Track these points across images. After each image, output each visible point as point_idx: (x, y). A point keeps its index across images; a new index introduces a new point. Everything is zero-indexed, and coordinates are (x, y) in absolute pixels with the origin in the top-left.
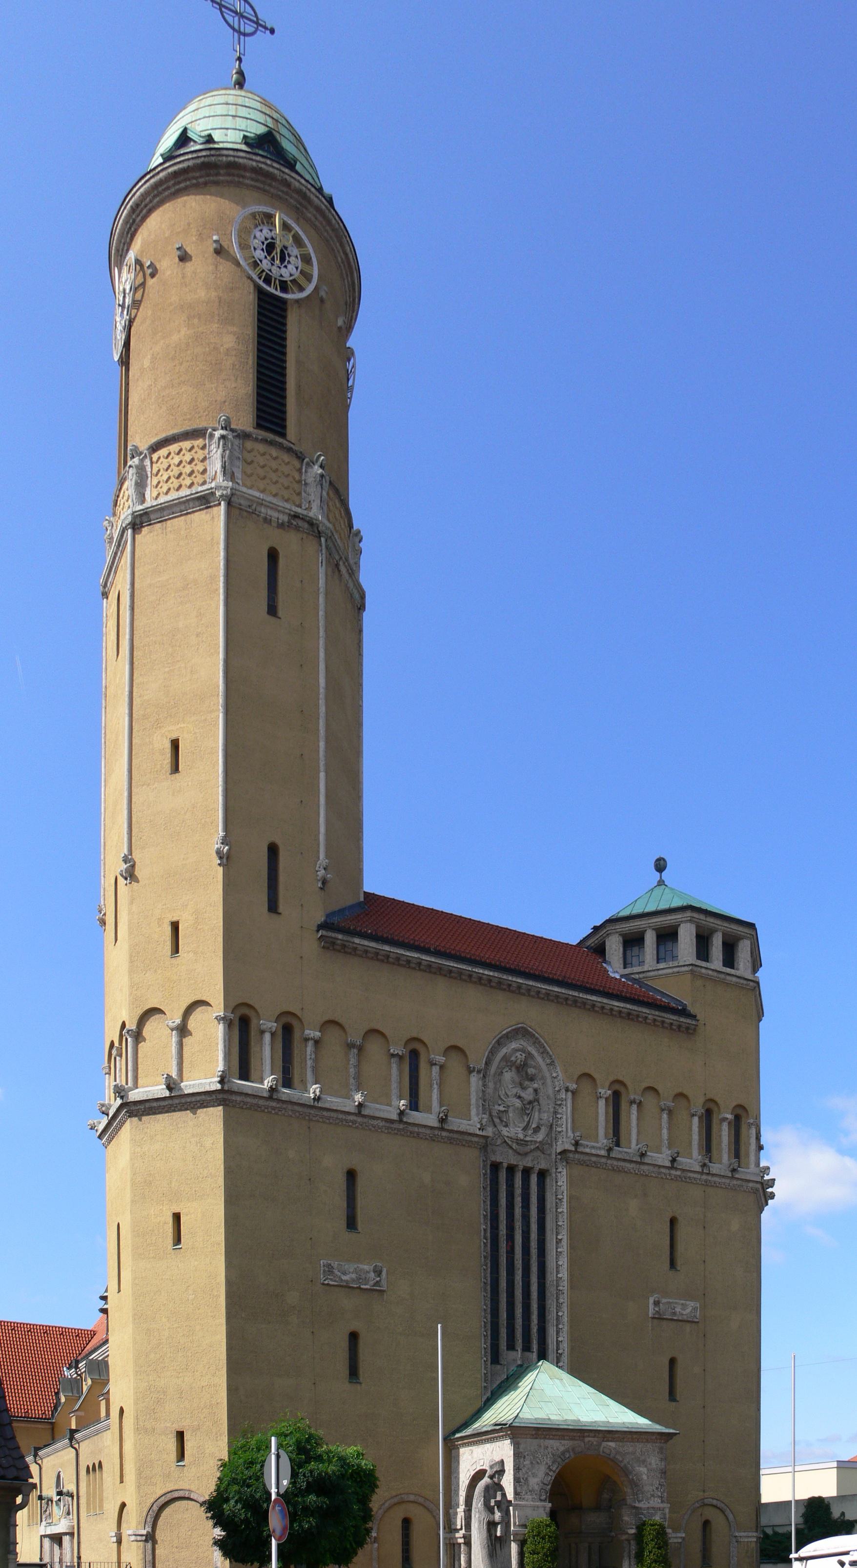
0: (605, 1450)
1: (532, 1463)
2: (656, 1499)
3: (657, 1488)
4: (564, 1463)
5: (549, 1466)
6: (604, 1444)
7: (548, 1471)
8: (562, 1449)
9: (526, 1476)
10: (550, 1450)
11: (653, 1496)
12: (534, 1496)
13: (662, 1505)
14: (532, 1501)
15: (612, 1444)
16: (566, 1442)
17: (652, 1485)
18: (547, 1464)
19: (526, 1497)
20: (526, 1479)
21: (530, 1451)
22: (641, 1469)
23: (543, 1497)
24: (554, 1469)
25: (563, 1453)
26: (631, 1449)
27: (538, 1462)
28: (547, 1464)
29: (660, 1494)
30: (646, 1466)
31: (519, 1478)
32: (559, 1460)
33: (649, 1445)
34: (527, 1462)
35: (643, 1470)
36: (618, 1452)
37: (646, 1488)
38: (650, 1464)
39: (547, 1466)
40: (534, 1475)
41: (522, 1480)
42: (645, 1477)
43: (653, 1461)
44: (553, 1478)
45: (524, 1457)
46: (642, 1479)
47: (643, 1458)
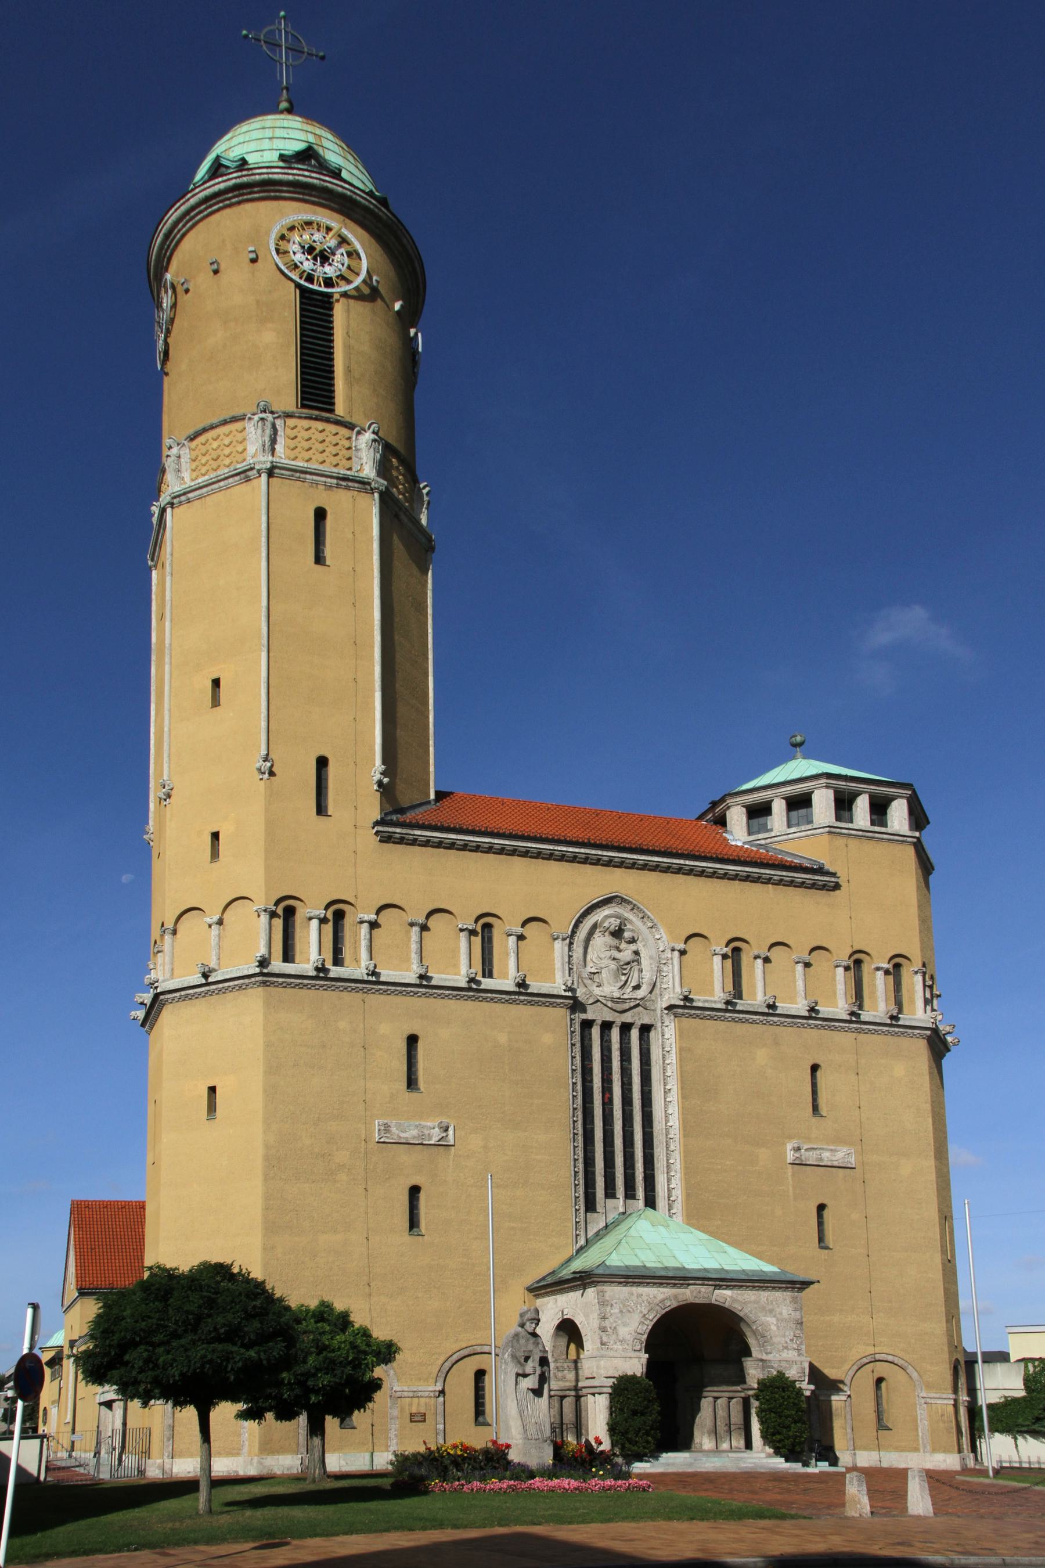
0: (718, 1299)
1: (621, 1312)
2: (790, 1352)
3: (792, 1340)
4: (664, 1312)
5: (645, 1315)
6: (716, 1291)
7: (642, 1320)
8: (661, 1297)
9: (614, 1325)
10: (645, 1298)
11: (786, 1348)
12: (626, 1346)
13: (798, 1359)
14: (623, 1351)
15: (728, 1293)
16: (665, 1290)
17: (784, 1336)
18: (641, 1312)
19: (615, 1347)
20: (615, 1328)
21: (619, 1299)
22: (768, 1319)
23: (638, 1347)
24: (651, 1318)
25: (662, 1301)
26: (753, 1298)
27: (629, 1311)
28: (641, 1312)
29: (795, 1346)
30: (774, 1316)
31: (605, 1327)
32: (658, 1308)
33: (778, 1294)
34: (616, 1310)
35: (771, 1320)
36: (734, 1300)
37: (775, 1340)
38: (781, 1314)
39: (641, 1315)
40: (625, 1325)
41: (609, 1329)
42: (774, 1328)
43: (784, 1311)
44: (650, 1327)
45: (612, 1305)
46: (770, 1329)
47: (771, 1307)
